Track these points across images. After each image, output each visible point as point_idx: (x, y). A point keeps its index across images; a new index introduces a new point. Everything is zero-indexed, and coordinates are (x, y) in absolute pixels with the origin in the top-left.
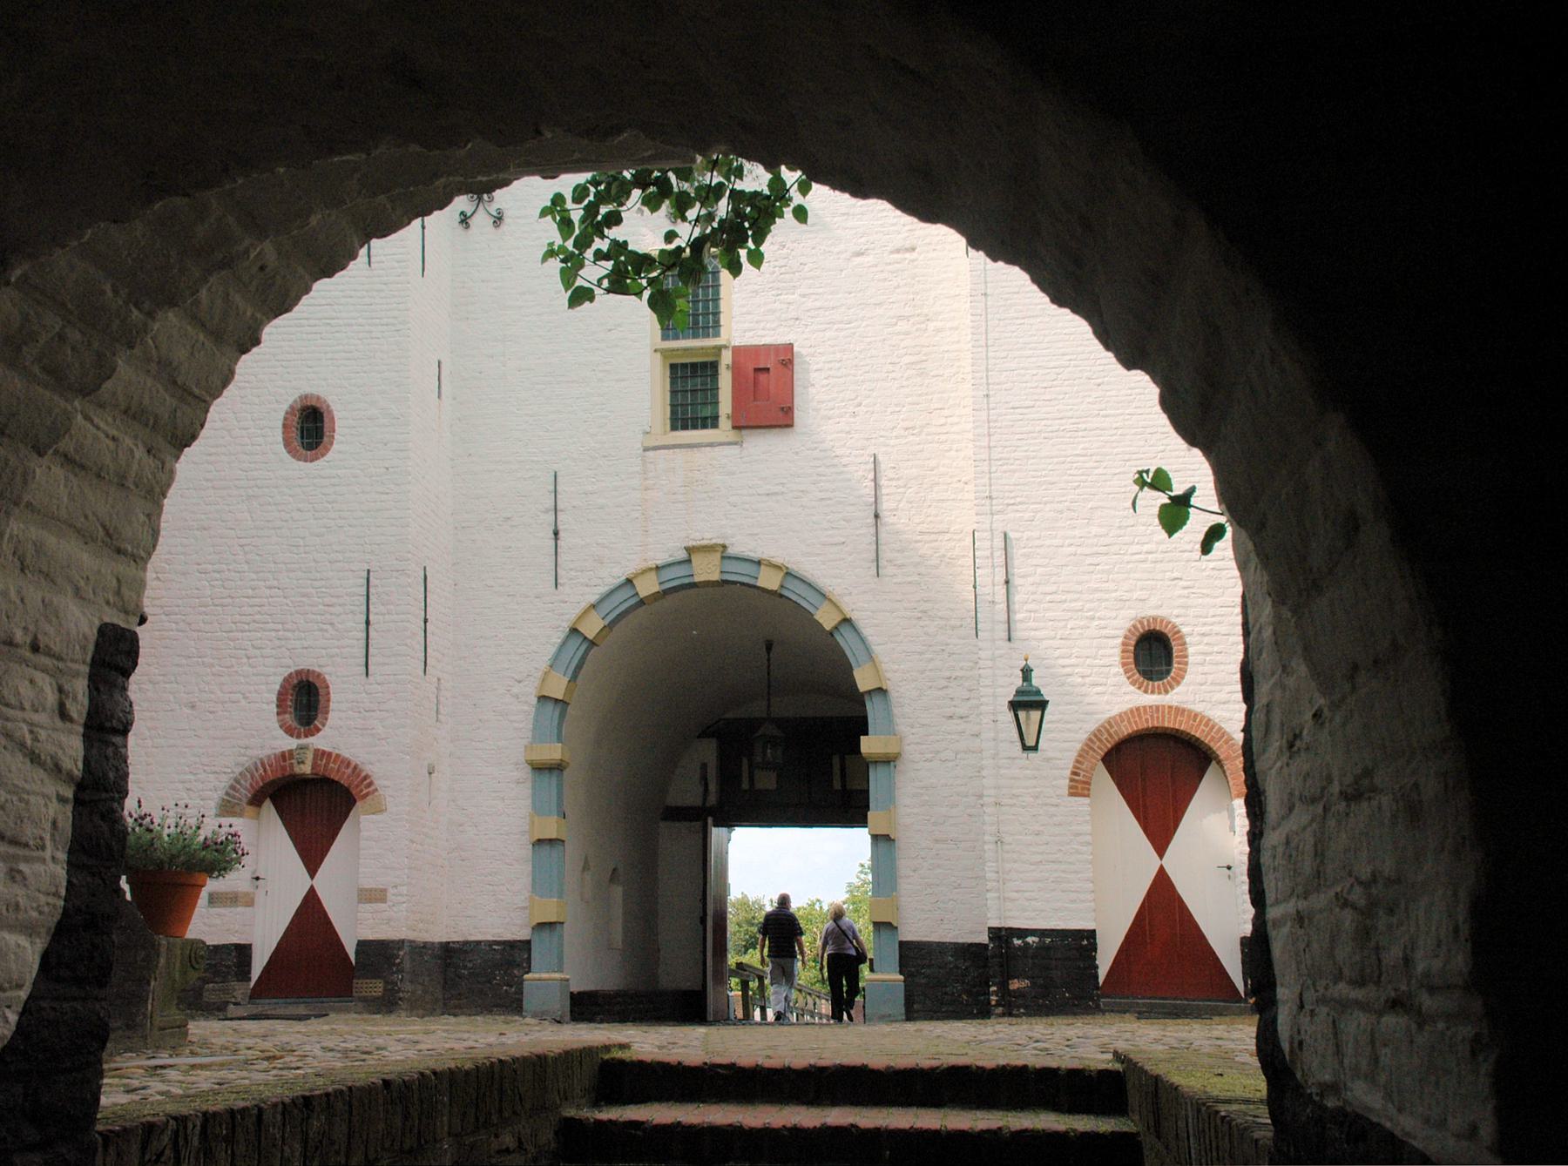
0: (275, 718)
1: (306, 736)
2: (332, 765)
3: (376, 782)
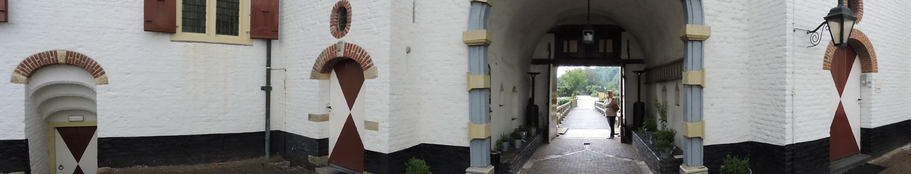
0: (329, 28)
1: (342, 37)
2: (352, 51)
3: (373, 60)
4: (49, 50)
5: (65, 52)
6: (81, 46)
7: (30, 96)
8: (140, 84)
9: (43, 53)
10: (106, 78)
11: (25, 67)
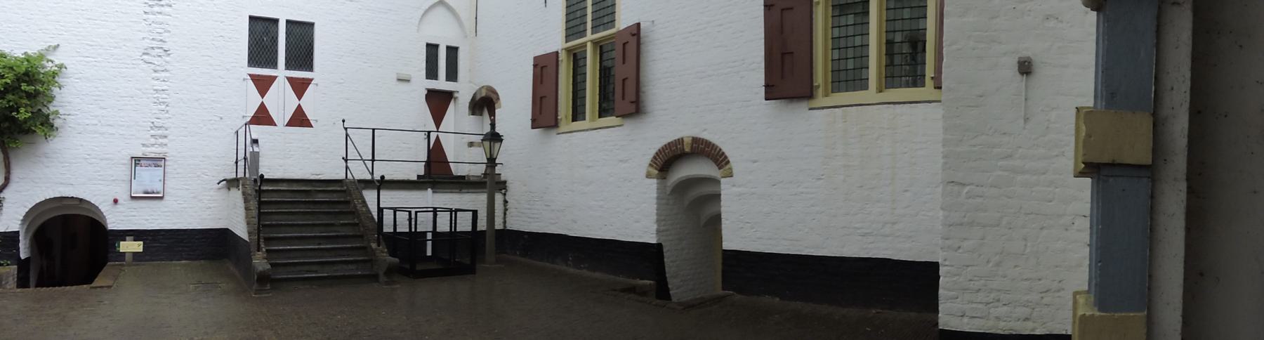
4: (676, 138)
5: (691, 138)
6: (705, 130)
7: (668, 193)
8: (770, 176)
9: (672, 142)
10: (731, 169)
11: (657, 160)
